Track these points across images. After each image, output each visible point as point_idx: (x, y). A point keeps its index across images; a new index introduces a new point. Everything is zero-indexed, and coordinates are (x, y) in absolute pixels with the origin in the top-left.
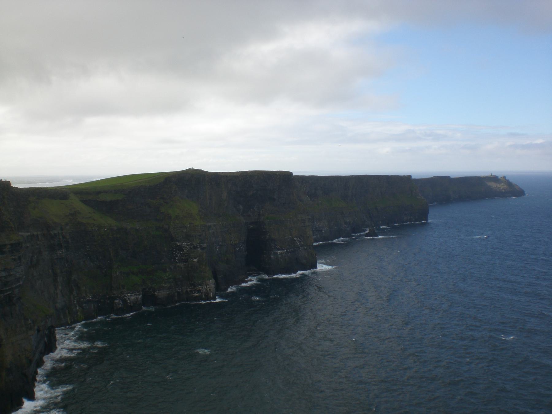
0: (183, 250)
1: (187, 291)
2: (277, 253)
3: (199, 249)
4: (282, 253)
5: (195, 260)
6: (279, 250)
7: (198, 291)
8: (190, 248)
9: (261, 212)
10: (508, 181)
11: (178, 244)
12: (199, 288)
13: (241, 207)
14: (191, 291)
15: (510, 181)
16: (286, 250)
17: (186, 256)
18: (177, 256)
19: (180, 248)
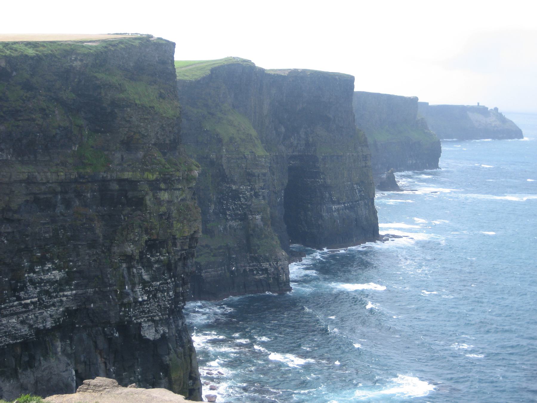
0: (239, 198)
1: (245, 271)
2: (331, 208)
3: (261, 198)
4: (338, 210)
5: (258, 217)
6: (334, 203)
7: (262, 270)
8: (251, 195)
9: (311, 140)
10: (501, 114)
11: (234, 187)
12: (265, 265)
13: (283, 129)
14: (251, 271)
15: (503, 114)
16: (344, 203)
17: (243, 209)
18: (229, 209)
19: (236, 195)
